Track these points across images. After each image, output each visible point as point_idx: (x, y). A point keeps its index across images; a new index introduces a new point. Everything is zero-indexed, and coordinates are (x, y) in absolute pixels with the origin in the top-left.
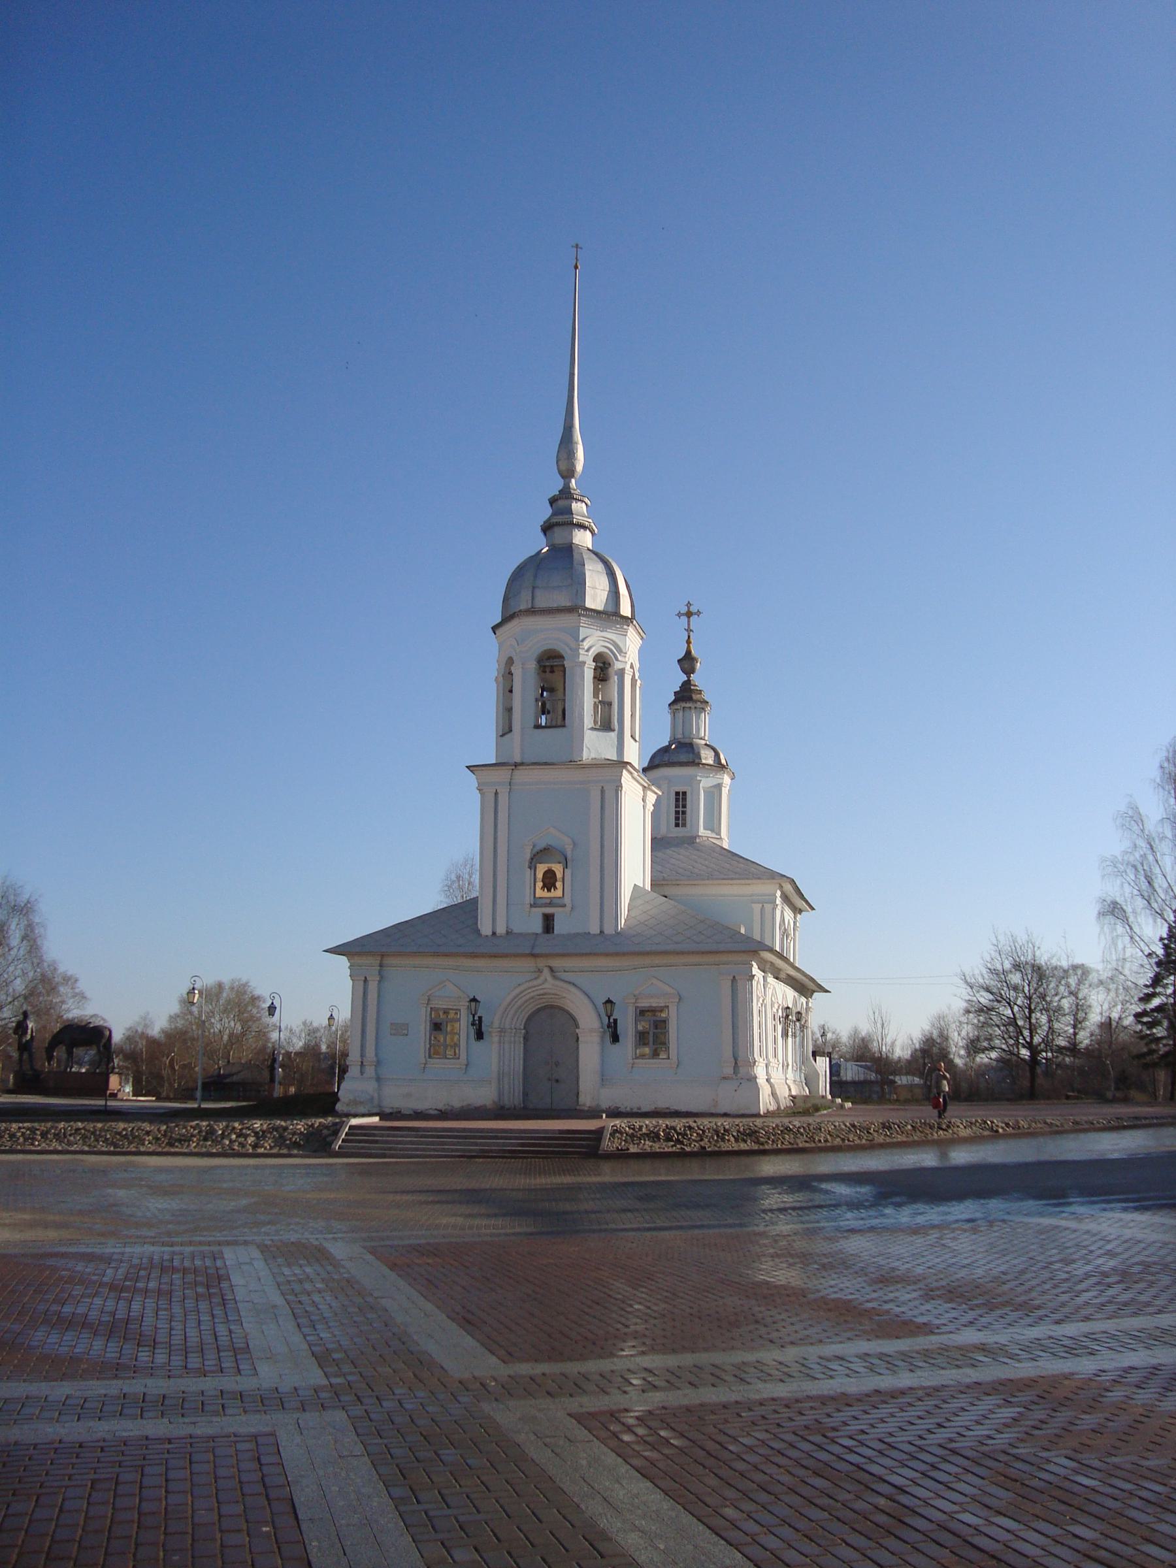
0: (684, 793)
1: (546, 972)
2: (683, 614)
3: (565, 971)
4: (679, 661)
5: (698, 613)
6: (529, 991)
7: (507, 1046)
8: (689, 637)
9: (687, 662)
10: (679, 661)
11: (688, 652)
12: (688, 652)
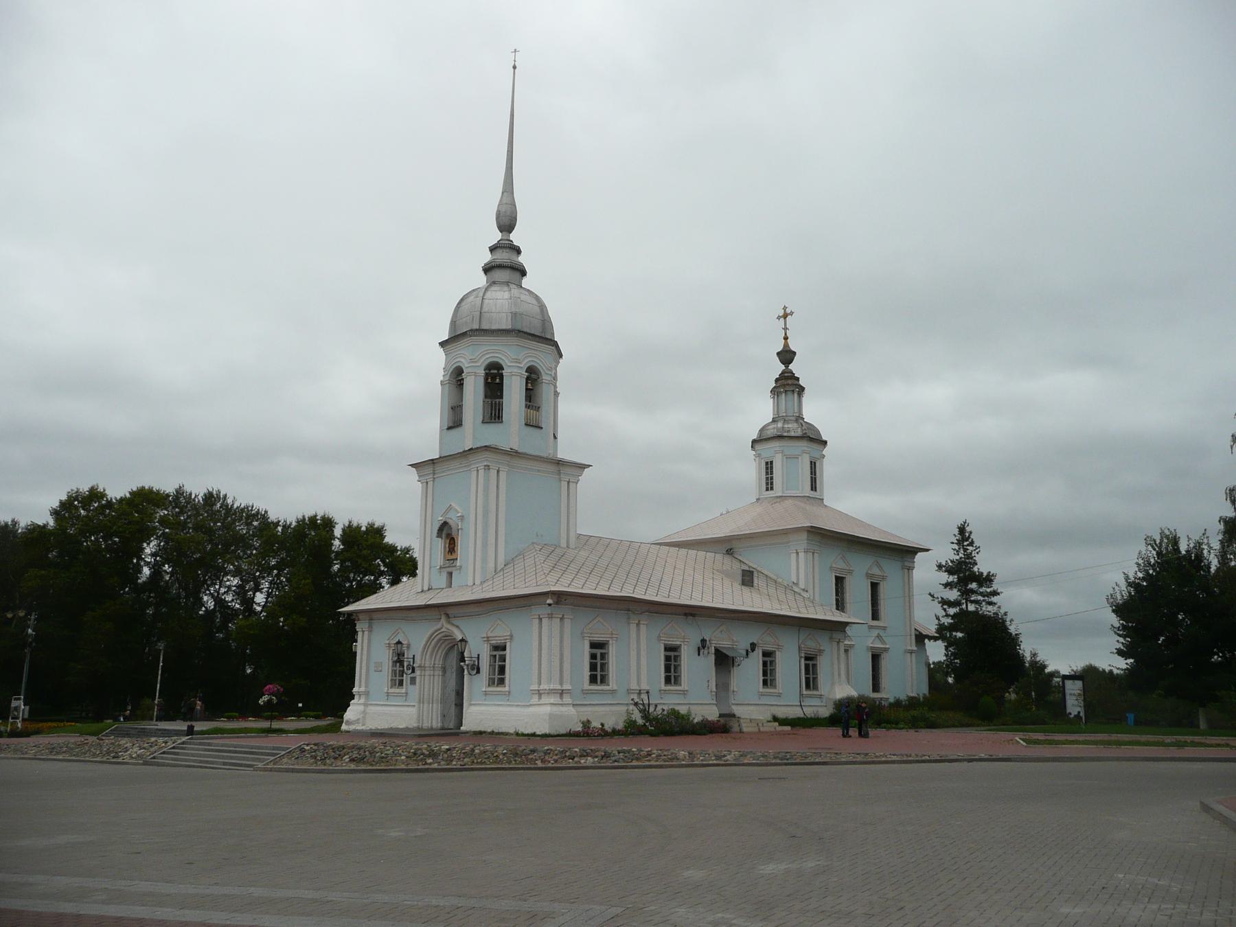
0: (772, 462)
2: (781, 317)
4: (778, 354)
5: (792, 313)
6: (436, 634)
7: (427, 678)
8: (786, 334)
9: (787, 356)
10: (778, 354)
11: (786, 345)
12: (786, 345)
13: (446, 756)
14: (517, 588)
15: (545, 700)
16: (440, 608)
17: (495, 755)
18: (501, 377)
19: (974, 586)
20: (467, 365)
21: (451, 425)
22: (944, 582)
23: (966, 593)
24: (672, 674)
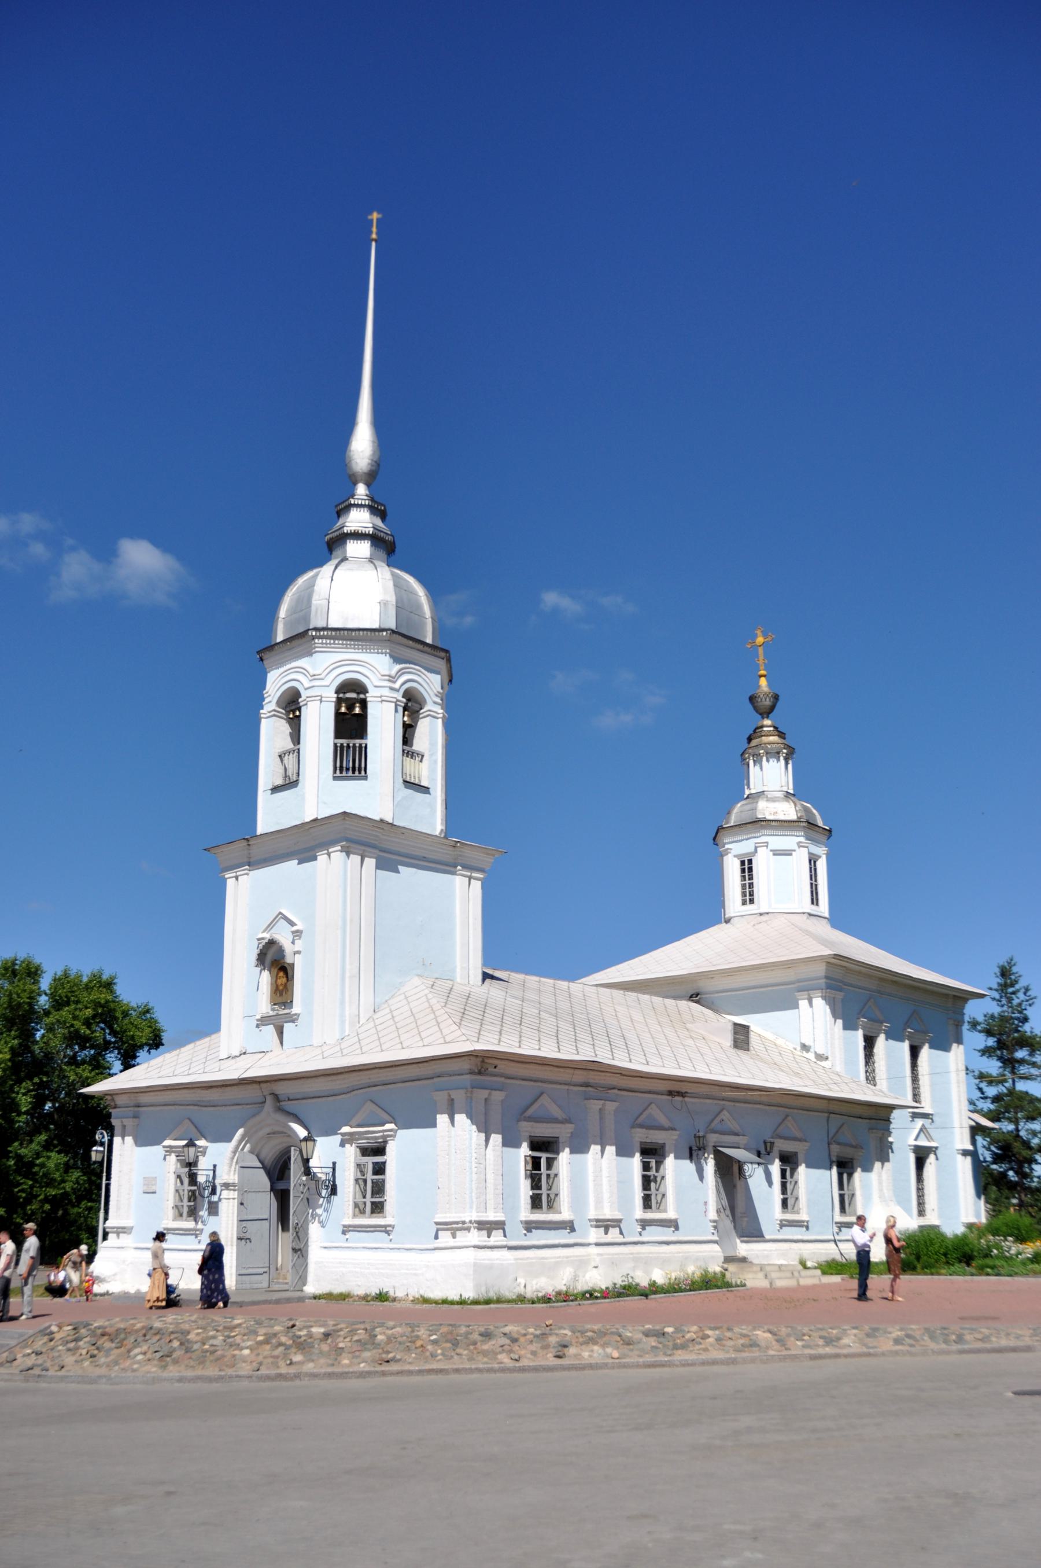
0: (750, 861)
1: (269, 1101)
3: (289, 1100)
13: (325, 1347)
14: (408, 1047)
15: (463, 1238)
16: (262, 1085)
17: (419, 1343)
18: (364, 704)
19: (1021, 1054)
20: (307, 685)
21: (279, 781)
22: (982, 1046)
23: (1010, 1063)
24: (544, 1191)
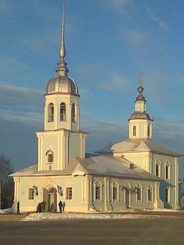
1: (49, 179)
